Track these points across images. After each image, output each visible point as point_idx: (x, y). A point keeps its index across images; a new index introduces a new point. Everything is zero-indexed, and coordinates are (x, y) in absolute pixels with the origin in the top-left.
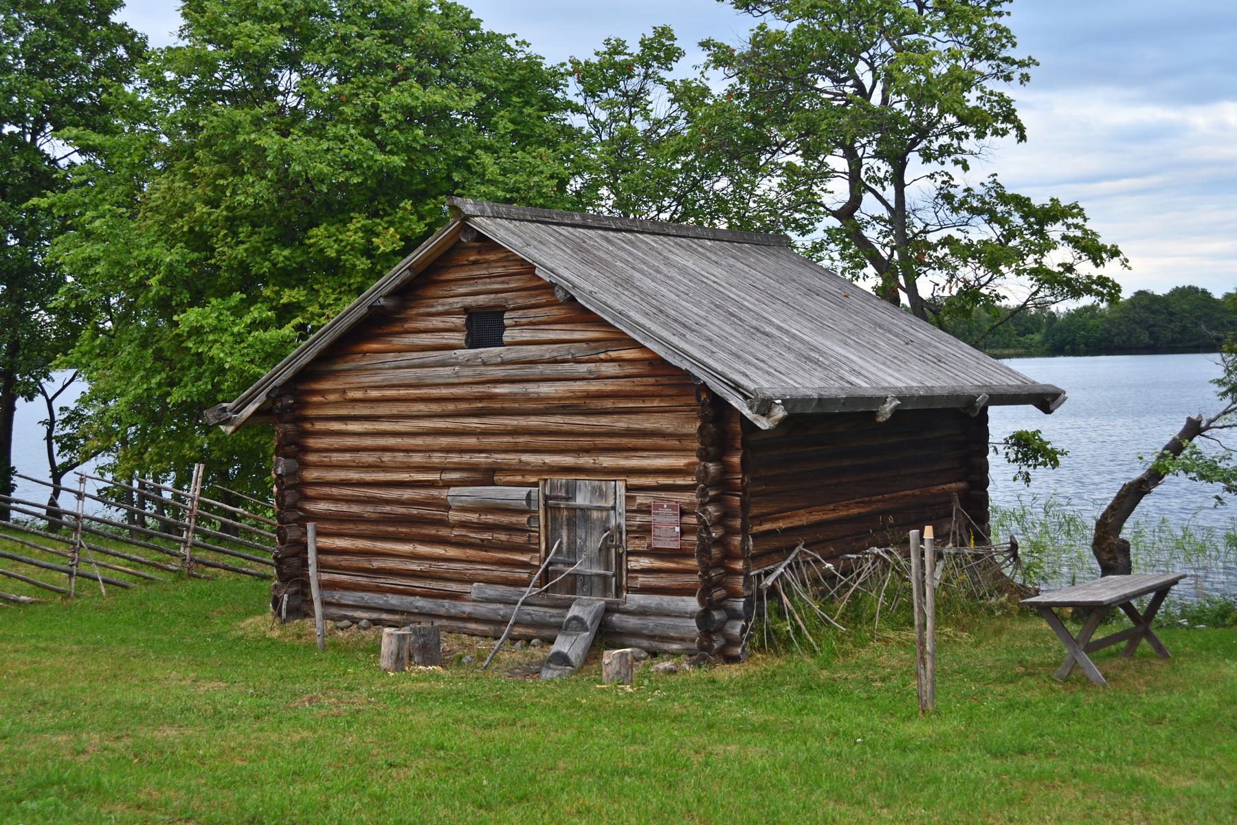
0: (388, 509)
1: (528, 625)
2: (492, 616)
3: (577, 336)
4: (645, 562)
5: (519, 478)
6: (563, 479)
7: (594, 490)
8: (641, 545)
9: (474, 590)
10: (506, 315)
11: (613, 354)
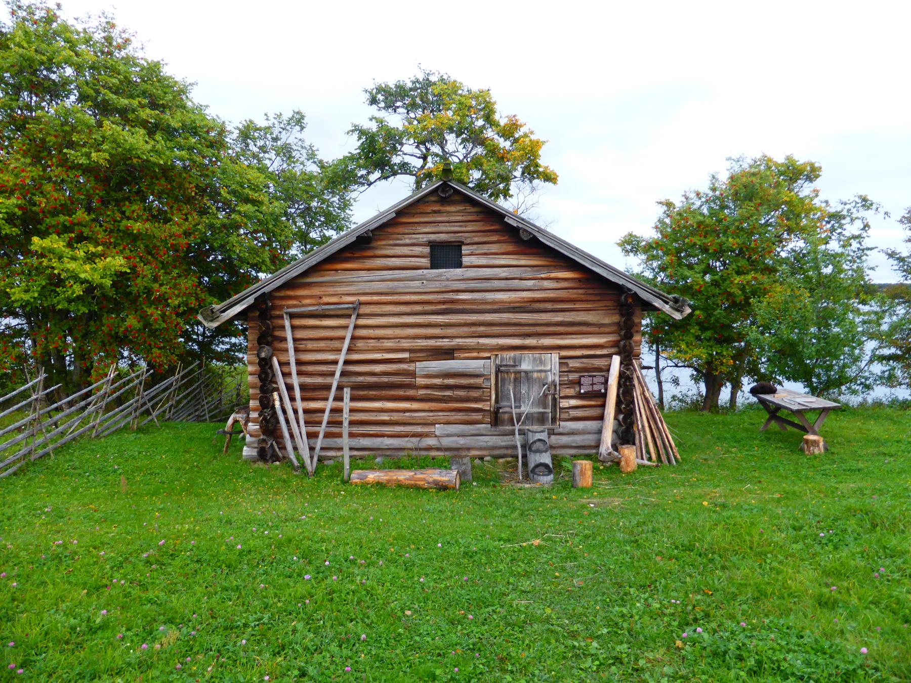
0: (361, 379)
1: (481, 449)
2: (454, 445)
3: (522, 262)
4: (573, 402)
5: (475, 354)
6: (512, 354)
7: (535, 360)
8: (571, 392)
9: (438, 429)
10: (464, 248)
11: (553, 275)
